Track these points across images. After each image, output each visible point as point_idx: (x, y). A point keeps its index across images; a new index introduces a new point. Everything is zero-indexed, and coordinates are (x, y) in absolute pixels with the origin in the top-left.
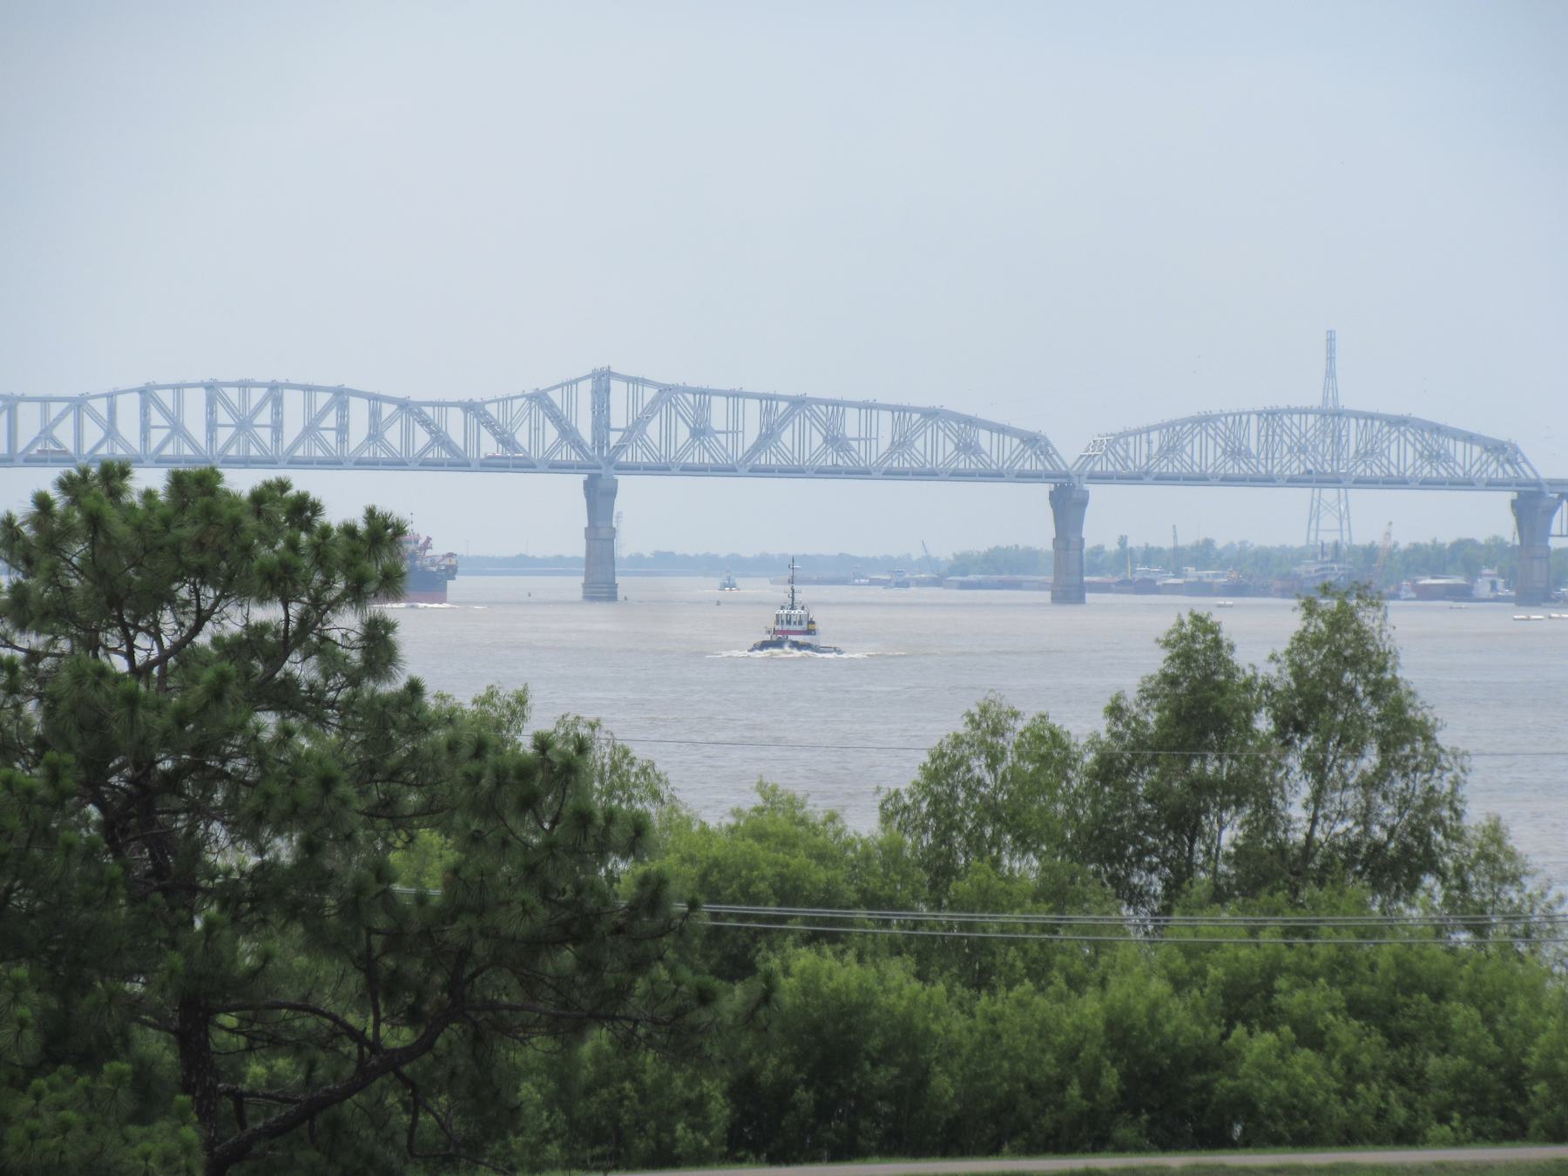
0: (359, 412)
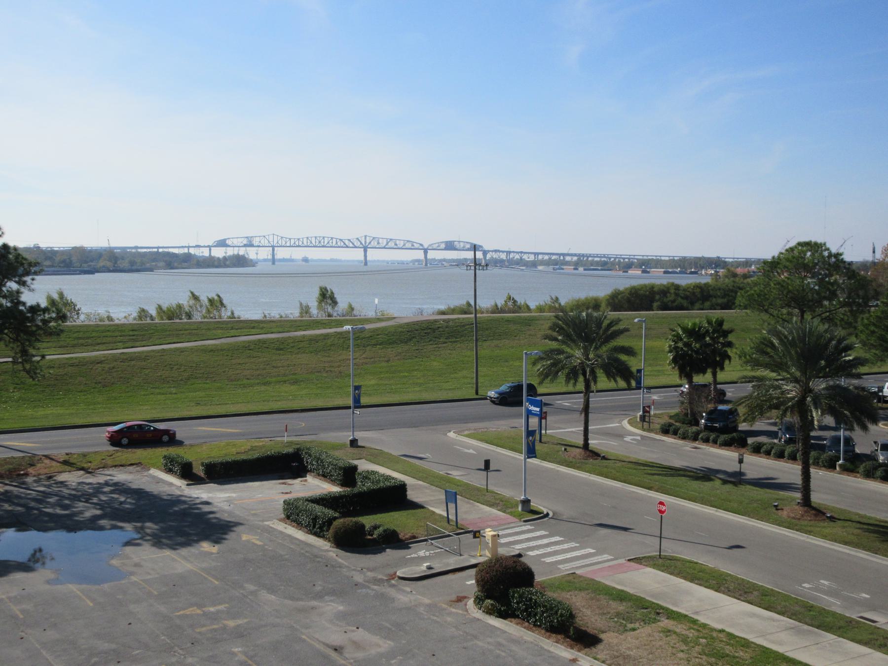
0: (335, 240)
